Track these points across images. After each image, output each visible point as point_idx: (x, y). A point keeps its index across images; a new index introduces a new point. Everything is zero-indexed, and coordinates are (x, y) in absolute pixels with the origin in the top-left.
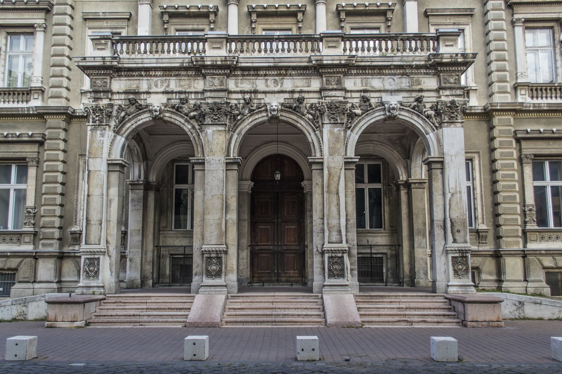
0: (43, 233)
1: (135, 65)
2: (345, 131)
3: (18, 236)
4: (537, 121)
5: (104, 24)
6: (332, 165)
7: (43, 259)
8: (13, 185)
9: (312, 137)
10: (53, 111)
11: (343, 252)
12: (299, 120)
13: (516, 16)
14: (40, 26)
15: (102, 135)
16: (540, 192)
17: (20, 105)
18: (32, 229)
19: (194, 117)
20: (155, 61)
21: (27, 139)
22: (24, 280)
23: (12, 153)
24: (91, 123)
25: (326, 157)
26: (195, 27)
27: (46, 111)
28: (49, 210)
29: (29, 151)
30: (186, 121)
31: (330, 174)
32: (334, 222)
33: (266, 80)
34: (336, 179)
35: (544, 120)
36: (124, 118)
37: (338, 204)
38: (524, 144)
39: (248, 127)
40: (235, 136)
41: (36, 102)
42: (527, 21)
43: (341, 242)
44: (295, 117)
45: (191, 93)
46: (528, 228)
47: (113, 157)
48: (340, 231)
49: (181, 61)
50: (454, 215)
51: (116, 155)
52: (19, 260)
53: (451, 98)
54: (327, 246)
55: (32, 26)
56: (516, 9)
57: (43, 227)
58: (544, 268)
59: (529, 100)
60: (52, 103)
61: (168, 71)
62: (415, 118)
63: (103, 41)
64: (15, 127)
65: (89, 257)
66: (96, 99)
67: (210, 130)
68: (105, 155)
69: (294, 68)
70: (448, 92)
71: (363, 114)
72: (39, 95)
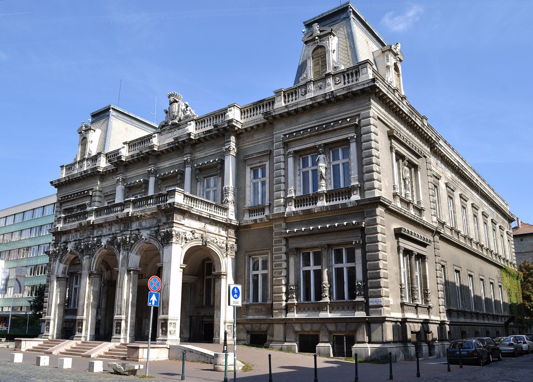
4: (301, 223)
9: (118, 258)
13: (290, 150)
16: (307, 274)
39: (99, 255)
40: (93, 260)
42: (295, 152)
46: (289, 302)
50: (164, 299)
58: (296, 332)
67: (84, 258)
68: (56, 273)
69: (113, 221)
71: (135, 242)
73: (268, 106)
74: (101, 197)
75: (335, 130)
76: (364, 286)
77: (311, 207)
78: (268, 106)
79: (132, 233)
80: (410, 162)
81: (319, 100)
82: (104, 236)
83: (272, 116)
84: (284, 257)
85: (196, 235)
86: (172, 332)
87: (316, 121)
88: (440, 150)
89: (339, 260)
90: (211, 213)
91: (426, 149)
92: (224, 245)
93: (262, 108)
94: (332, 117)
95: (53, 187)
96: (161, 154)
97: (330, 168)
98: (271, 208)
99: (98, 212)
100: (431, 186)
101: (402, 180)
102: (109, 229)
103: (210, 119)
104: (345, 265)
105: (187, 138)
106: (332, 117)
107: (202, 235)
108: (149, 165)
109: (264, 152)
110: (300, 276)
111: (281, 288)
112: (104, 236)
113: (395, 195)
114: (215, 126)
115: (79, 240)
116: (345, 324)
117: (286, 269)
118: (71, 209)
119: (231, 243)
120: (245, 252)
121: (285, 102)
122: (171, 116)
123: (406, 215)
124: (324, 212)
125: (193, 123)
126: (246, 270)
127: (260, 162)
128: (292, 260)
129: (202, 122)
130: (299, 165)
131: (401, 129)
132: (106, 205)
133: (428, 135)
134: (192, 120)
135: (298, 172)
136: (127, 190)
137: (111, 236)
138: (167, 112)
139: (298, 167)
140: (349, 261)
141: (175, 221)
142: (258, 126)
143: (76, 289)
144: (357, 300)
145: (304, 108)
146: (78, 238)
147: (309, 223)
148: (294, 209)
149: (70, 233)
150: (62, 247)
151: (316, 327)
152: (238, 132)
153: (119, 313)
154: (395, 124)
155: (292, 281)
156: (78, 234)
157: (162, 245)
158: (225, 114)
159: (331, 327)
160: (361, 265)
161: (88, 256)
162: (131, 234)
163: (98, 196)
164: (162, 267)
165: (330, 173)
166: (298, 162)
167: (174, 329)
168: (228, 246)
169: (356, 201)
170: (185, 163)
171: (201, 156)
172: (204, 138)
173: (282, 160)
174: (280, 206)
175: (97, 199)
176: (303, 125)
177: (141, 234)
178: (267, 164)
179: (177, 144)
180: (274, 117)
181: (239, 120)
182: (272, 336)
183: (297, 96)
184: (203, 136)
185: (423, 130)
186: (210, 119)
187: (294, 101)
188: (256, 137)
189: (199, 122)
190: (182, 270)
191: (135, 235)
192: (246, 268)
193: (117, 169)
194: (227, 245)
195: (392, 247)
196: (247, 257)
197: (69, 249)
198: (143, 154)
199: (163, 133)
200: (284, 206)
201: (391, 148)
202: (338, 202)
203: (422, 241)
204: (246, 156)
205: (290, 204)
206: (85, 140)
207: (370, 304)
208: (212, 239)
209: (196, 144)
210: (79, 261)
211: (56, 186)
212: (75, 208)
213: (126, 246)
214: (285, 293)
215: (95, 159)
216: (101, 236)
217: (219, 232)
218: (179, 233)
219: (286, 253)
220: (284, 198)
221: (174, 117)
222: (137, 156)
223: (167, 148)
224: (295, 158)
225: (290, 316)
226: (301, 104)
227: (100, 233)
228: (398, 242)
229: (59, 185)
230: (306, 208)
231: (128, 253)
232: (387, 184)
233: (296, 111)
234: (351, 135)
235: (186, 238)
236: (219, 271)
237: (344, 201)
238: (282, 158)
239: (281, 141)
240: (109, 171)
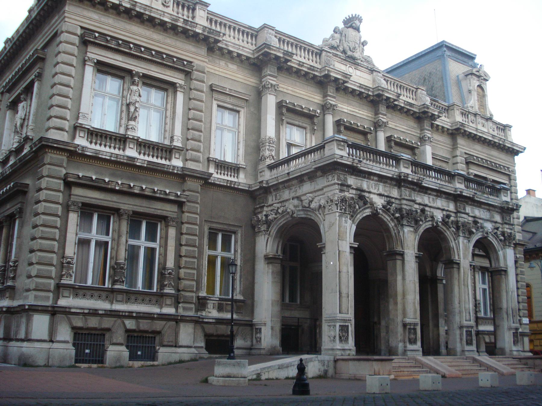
0: (185, 297)
1: (367, 169)
3: (159, 298)
5: (228, 99)
7: (184, 323)
8: (142, 243)
9: (453, 244)
10: (198, 175)
12: (447, 231)
17: (163, 162)
18: (173, 292)
19: (397, 218)
20: (379, 169)
21: (173, 198)
22: (170, 344)
23: (153, 210)
24: (339, 211)
25: (462, 260)
26: (301, 124)
27: (192, 174)
28: (190, 273)
29: (169, 210)
30: (392, 219)
31: (464, 273)
32: (467, 306)
33: (429, 197)
37: (468, 294)
41: (177, 162)
43: (470, 321)
44: (445, 228)
48: (470, 313)
49: (393, 173)
52: (164, 323)
54: (465, 323)
55: (173, 85)
56: (471, 166)
57: (183, 290)
60: (191, 165)
61: (382, 178)
62: (494, 240)
63: (342, 143)
64: (152, 183)
65: (342, 324)
66: (341, 191)
67: (406, 229)
72: (180, 156)
149: (369, 179)
153: (468, 318)
172: (402, 108)
184: (403, 105)
212: (138, 73)
222: (309, 69)
226: (486, 135)
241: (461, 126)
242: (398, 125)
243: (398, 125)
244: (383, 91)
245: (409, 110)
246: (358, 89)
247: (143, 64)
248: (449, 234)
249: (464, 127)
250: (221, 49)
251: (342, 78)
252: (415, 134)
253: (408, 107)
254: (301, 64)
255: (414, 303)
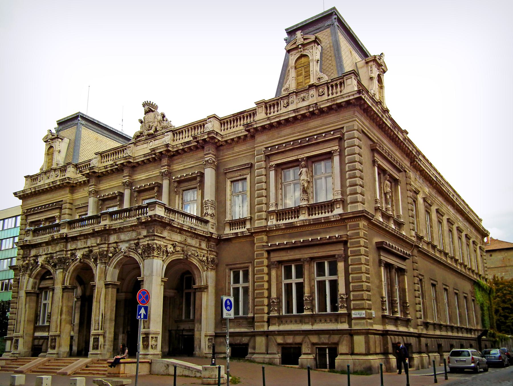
2: (106, 267)
4: (283, 236)
6: (99, 286)
9: (94, 272)
11: (99, 335)
14: (57, 217)
15: (24, 279)
31: (98, 291)
34: (100, 294)
35: (287, 235)
36: (32, 268)
37: (99, 308)
38: (272, 255)
40: (67, 274)
42: (278, 165)
44: (89, 261)
45: (54, 253)
46: (271, 315)
47: (28, 289)
48: (99, 324)
51: (30, 288)
53: (146, 243)
59: (275, 222)
67: (57, 272)
68: (25, 289)
69: (89, 234)
70: (148, 239)
71: (113, 256)
73: (249, 117)
74: (71, 209)
75: (318, 143)
76: (346, 298)
77: (293, 220)
78: (249, 117)
79: (110, 246)
80: (391, 176)
81: (302, 112)
82: (79, 249)
83: (254, 128)
84: (266, 270)
85: (178, 249)
86: (154, 346)
87: (298, 134)
88: (419, 164)
89: (321, 272)
90: (192, 226)
91: (406, 163)
92: (205, 258)
93: (242, 120)
94: (315, 129)
95: (17, 198)
96: (137, 165)
97: (312, 182)
98: (252, 222)
99: (71, 224)
100: (410, 200)
101: (383, 194)
102: (85, 242)
103: (188, 131)
104: (327, 278)
105: (165, 149)
106: (315, 129)
107: (183, 248)
108: (124, 177)
109: (245, 165)
110: (282, 289)
111: (263, 301)
112: (79, 249)
113: (377, 209)
114: (195, 138)
115: (51, 253)
116: (327, 336)
117: (267, 281)
118: (38, 222)
119: (212, 256)
120: (227, 265)
121: (267, 114)
122: (147, 125)
123: (387, 229)
124: (307, 225)
125: (170, 134)
126: (227, 284)
127: (240, 175)
128: (273, 273)
129: (180, 133)
130: (281, 179)
131: (383, 142)
132: (77, 217)
133: (408, 149)
134: (169, 131)
135: (280, 186)
136: (100, 202)
137: (87, 250)
138: (141, 122)
139: (280, 181)
140: (331, 274)
141: (156, 234)
142: (239, 138)
143: (45, 305)
144: (339, 312)
145: (287, 121)
146: (50, 251)
147: (291, 236)
148: (275, 222)
150: (32, 261)
151: (298, 339)
152: (218, 144)
153: (96, 328)
154: (378, 137)
155: (274, 295)
156: (50, 247)
157: (142, 258)
158: (204, 126)
159: (314, 339)
160: (344, 278)
161: (62, 270)
162: (108, 247)
163: (69, 208)
164: (143, 281)
165: (313, 187)
166: (280, 175)
167: (155, 343)
168: (209, 260)
169: (340, 215)
170: (163, 175)
171: (180, 169)
172: (183, 150)
173: (264, 173)
174: (262, 219)
175: (67, 211)
176: (286, 137)
177: (119, 247)
178: (248, 177)
179: (154, 156)
180: (256, 129)
181: (219, 131)
182: (254, 348)
183: (279, 108)
184: (181, 148)
185: (404, 144)
186: (188, 131)
187: (276, 113)
188: (237, 149)
189: (177, 133)
190: (163, 284)
191: (113, 248)
192: (227, 281)
193: (88, 181)
194: (207, 259)
195: (374, 260)
196: (227, 271)
197: (39, 263)
198: (117, 165)
199: (138, 144)
200: (266, 219)
201: (374, 162)
202: (320, 216)
203: (402, 254)
204: (227, 169)
205: (272, 217)
206: (51, 150)
207: (353, 316)
208: (193, 252)
209: (174, 155)
210: (51, 274)
211: (20, 198)
213: (104, 258)
214: (267, 306)
215: (63, 169)
216: (75, 249)
217: (200, 245)
218: (160, 246)
219: (267, 266)
220: (265, 212)
221: (150, 128)
222: (111, 167)
223: (143, 159)
224: (276, 171)
225: (272, 328)
226: (284, 116)
227: (74, 247)
228: (380, 255)
229: (23, 196)
230: (288, 221)
231: (106, 267)
232: (370, 198)
233: (279, 123)
234: (334, 148)
235: (167, 251)
236: (200, 285)
237: (327, 215)
238: (263, 171)
239: (262, 154)
240: (80, 182)
241: (247, 127)
242: (185, 164)
243: (185, 164)
244: (154, 151)
245: (189, 148)
246: (144, 159)
247: (45, 214)
248: (92, 265)
249: (251, 126)
250: (76, 183)
251: (125, 161)
252: (227, 157)
253: (187, 146)
254: (106, 167)
255: (57, 321)
